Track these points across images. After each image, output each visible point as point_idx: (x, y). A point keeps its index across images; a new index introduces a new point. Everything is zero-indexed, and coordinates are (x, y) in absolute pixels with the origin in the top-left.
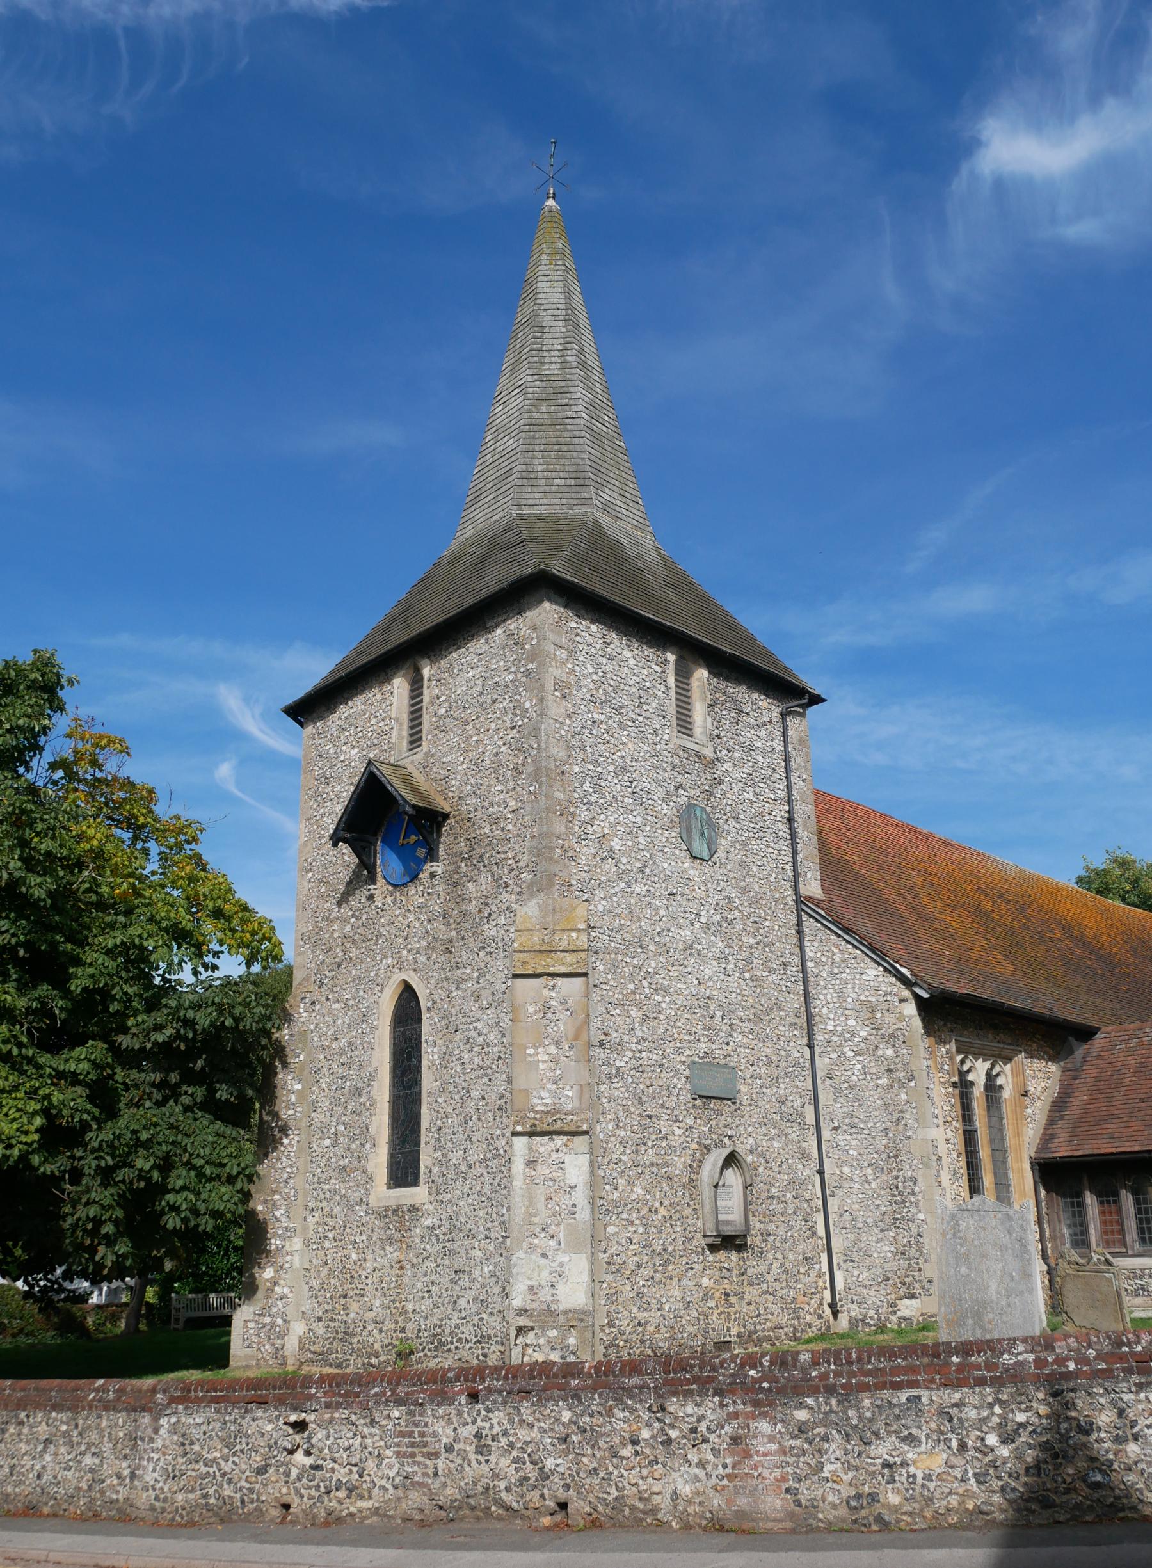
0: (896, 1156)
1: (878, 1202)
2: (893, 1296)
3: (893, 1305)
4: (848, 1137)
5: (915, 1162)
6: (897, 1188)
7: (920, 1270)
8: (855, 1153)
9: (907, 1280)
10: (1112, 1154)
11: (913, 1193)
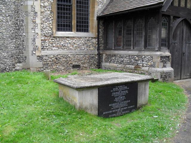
0: (18, 12)
1: (11, 29)
2: (14, 62)
3: (14, 65)
4: (2, 6)
5: (23, 14)
6: (17, 24)
7: (23, 53)
8: (4, 11)
9: (18, 57)
10: (117, 12)
11: (22, 26)
